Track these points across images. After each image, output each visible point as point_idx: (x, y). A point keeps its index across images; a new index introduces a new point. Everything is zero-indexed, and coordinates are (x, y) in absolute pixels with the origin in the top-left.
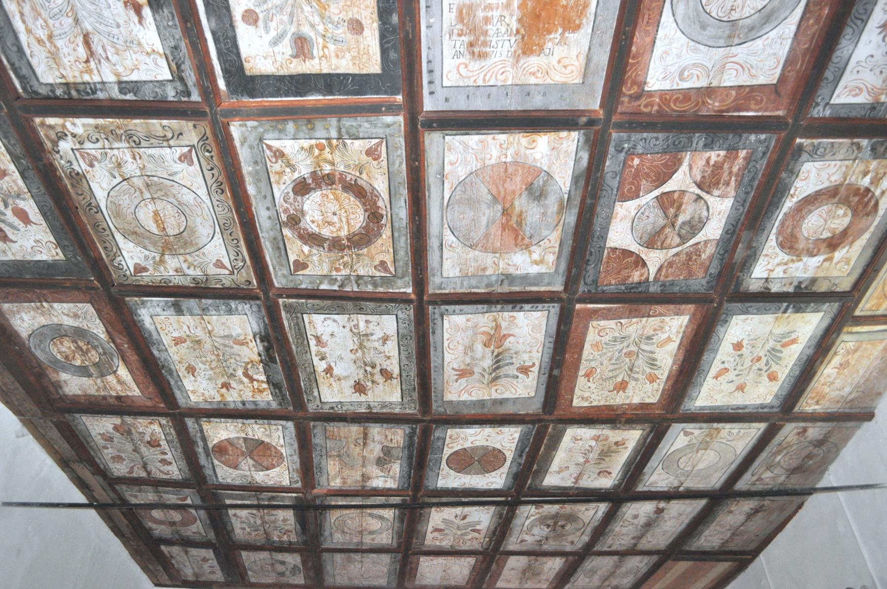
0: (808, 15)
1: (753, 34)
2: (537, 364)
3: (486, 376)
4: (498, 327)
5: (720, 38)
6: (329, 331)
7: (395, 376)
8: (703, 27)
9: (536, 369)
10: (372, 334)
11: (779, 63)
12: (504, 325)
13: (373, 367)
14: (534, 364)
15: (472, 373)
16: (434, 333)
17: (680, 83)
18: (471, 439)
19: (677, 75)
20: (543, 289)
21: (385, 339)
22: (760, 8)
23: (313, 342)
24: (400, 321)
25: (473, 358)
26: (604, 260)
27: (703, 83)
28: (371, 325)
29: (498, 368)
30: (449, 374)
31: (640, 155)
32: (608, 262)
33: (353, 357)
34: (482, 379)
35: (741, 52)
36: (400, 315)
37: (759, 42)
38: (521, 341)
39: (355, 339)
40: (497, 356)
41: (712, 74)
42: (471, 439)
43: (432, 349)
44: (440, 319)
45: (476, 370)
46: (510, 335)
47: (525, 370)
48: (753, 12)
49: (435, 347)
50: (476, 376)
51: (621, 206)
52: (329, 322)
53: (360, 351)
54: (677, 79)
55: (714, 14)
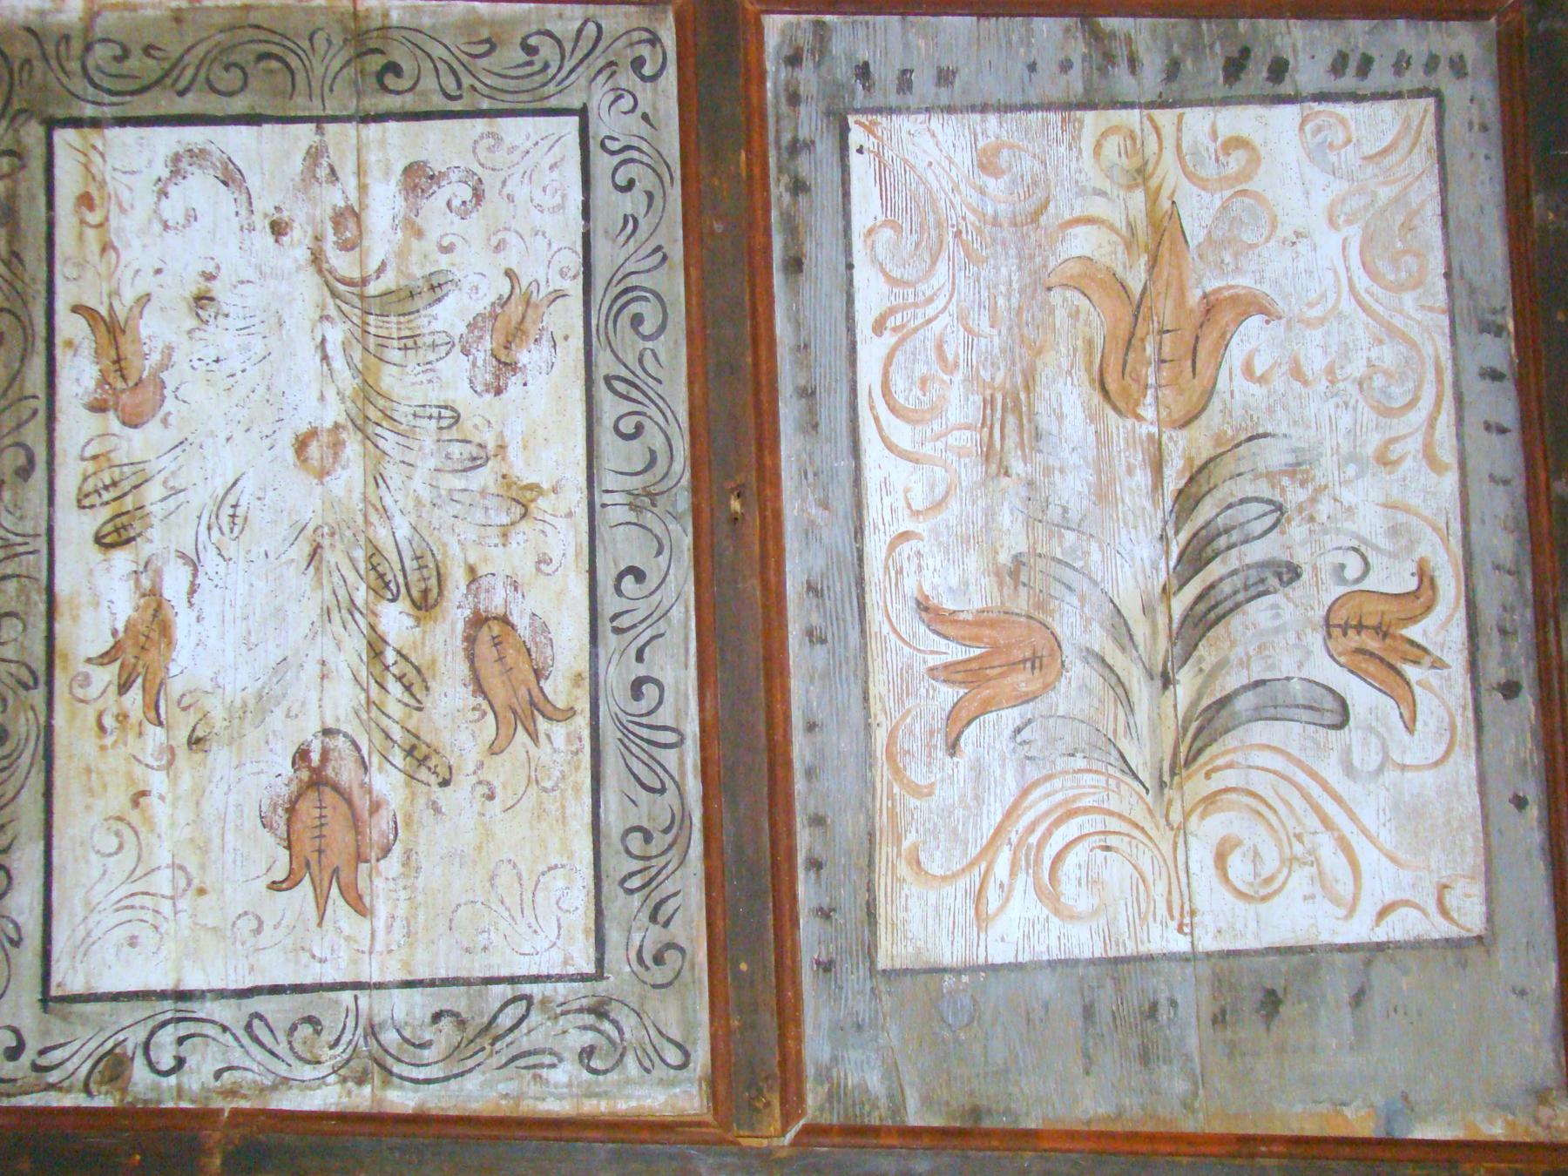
2: (1449, 587)
3: (1141, 690)
4: (1161, 236)
6: (185, 260)
7: (558, 689)
9: (1441, 630)
10: (436, 287)
12: (1197, 212)
13: (425, 605)
14: (1425, 576)
15: (1043, 659)
16: (795, 265)
21: (507, 330)
23: (79, 375)
24: (603, 164)
25: (1037, 506)
28: (434, 207)
29: (1204, 619)
30: (905, 661)
33: (305, 500)
34: (1112, 718)
36: (606, 123)
39: (336, 335)
40: (1187, 500)
43: (789, 412)
44: (825, 147)
45: (1076, 627)
46: (1252, 305)
47: (1374, 636)
49: (807, 393)
50: (1076, 688)
52: (199, 188)
53: (353, 447)
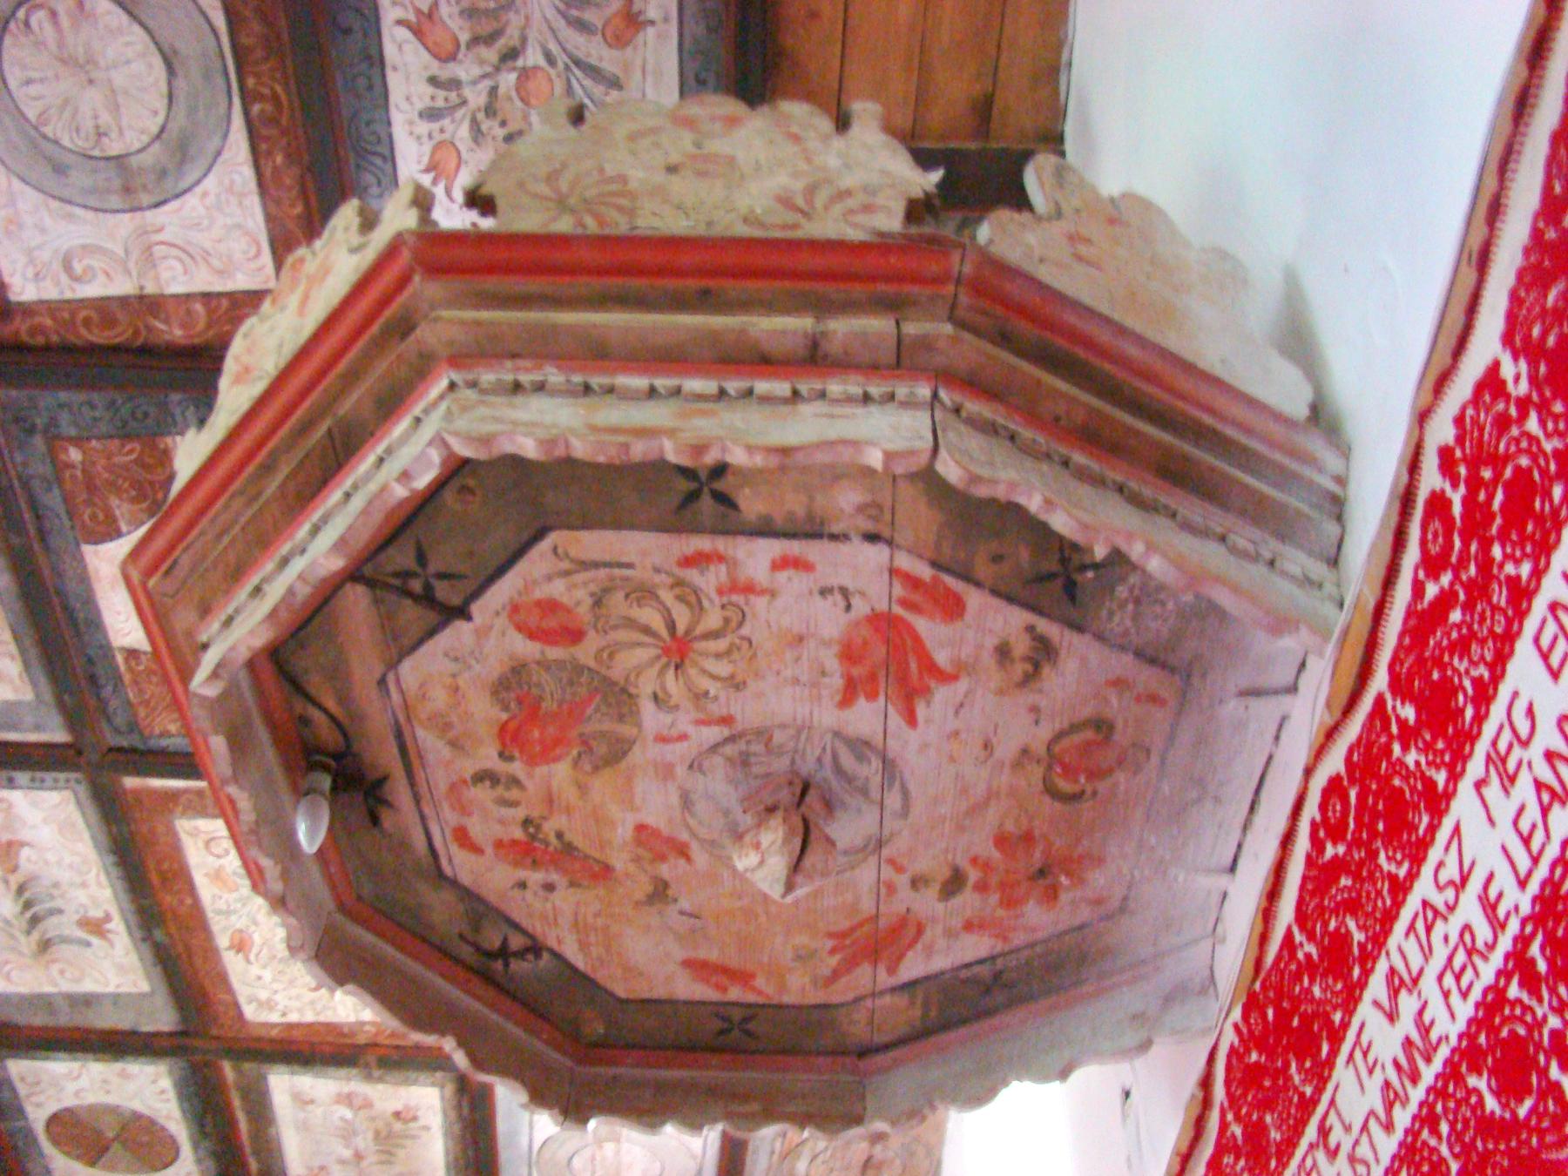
0: (264, 147)
1: (169, 185)
5: (109, 191)
8: (60, 170)
11: (258, 244)
17: (76, 286)
18: (71, 1087)
19: (57, 266)
20: (33, 737)
22: (155, 130)
26: (127, 678)
27: (122, 286)
31: (78, 442)
32: (136, 683)
35: (170, 220)
37: (192, 200)
38: (51, 857)
41: (131, 265)
42: (71, 1087)
48: (145, 139)
51: (96, 553)
54: (64, 278)
55: (66, 142)
